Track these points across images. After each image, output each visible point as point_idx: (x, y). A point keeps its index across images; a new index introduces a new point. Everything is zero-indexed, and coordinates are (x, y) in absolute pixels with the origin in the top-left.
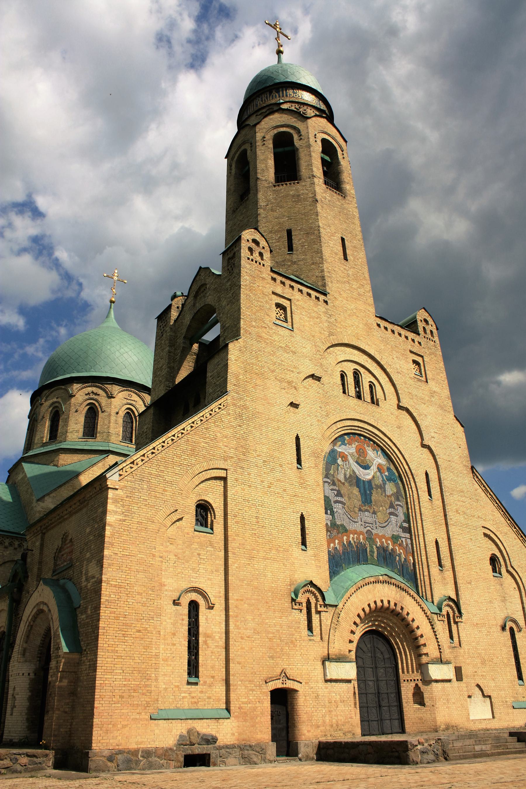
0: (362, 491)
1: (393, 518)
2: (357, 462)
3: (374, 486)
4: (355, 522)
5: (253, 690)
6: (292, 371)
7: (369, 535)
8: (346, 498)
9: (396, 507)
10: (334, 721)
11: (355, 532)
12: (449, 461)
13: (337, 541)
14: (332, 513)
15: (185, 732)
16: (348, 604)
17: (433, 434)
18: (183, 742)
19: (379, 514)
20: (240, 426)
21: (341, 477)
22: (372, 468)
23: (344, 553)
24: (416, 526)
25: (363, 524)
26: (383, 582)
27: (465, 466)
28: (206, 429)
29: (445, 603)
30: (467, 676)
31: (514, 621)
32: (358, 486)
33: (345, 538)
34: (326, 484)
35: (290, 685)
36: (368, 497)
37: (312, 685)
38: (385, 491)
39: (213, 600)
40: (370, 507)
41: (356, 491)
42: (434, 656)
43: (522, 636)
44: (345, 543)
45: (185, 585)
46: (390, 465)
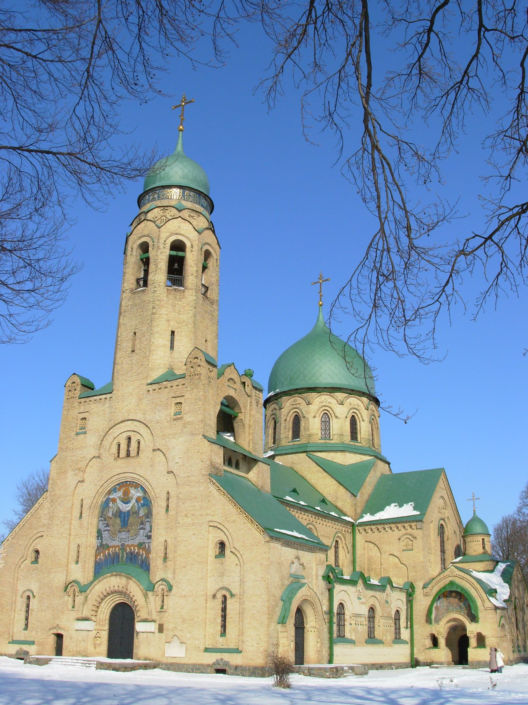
0: (122, 519)
1: (142, 531)
2: (123, 502)
3: (131, 513)
4: (114, 540)
5: (44, 634)
6: (82, 461)
7: (123, 546)
8: (111, 527)
9: (145, 524)
10: (78, 650)
11: (113, 546)
12: (189, 477)
13: (102, 554)
14: (101, 539)
15: (19, 649)
16: (94, 590)
17: (177, 461)
18: (18, 653)
19: (132, 531)
20: (51, 506)
21: (110, 514)
22: (132, 501)
23: (105, 561)
24: (153, 534)
25: (120, 540)
26: (116, 575)
27: (203, 475)
28: (37, 513)
29: (160, 583)
30: (168, 630)
31: (228, 590)
32: (120, 517)
33: (107, 551)
34: (101, 521)
35: (60, 632)
36: (126, 522)
37: (69, 632)
38: (139, 515)
39: (35, 594)
40: (126, 528)
41: (118, 521)
42: (145, 618)
43: (235, 601)
44: (107, 554)
45: (25, 589)
46: (145, 494)
